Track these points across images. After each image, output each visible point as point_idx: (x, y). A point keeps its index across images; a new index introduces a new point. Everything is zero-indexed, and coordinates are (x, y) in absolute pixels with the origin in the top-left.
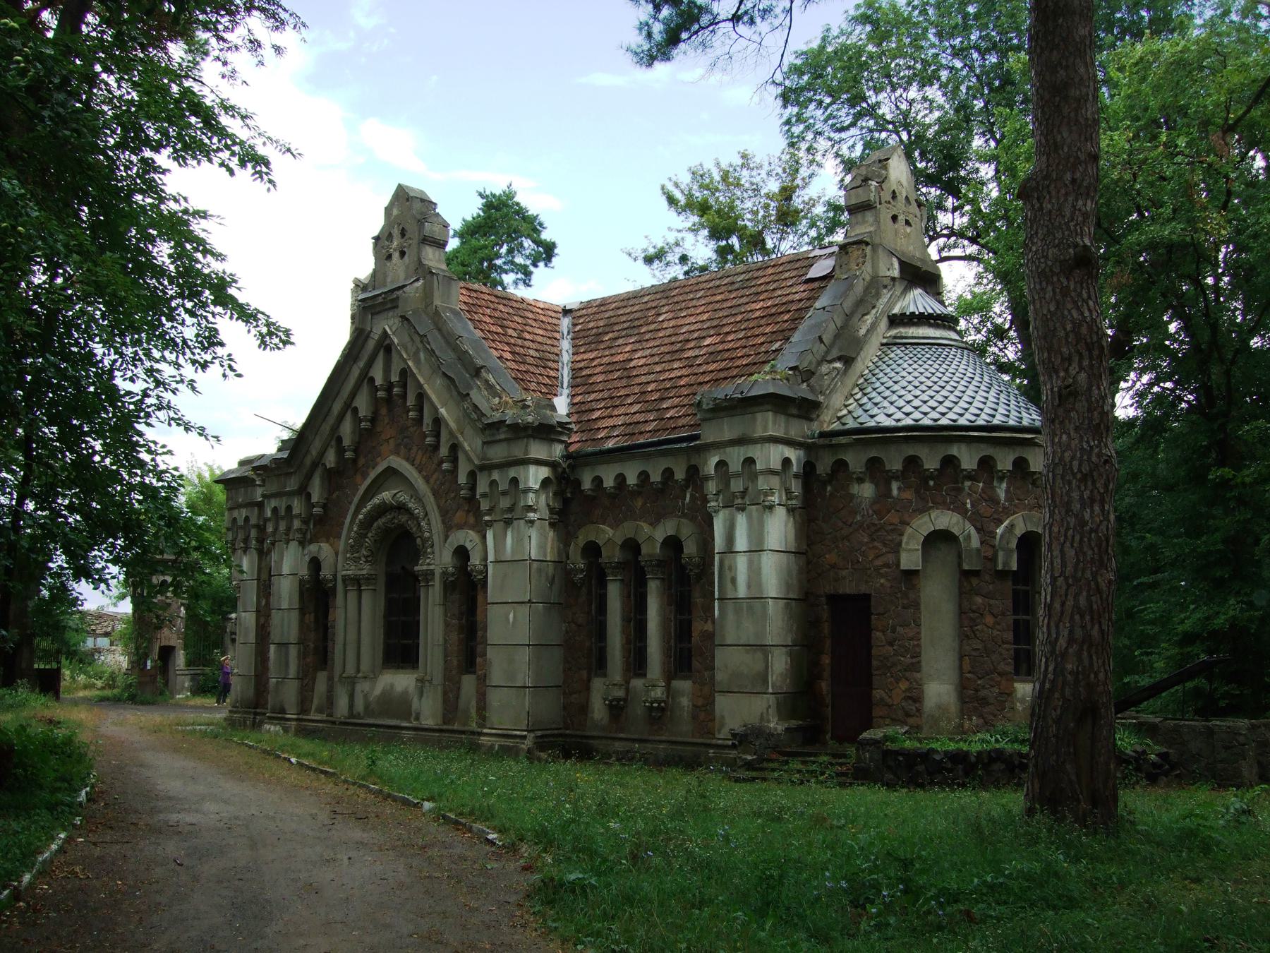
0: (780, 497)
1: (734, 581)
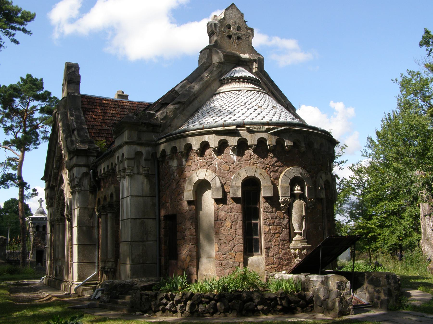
0: (138, 169)
1: (123, 210)
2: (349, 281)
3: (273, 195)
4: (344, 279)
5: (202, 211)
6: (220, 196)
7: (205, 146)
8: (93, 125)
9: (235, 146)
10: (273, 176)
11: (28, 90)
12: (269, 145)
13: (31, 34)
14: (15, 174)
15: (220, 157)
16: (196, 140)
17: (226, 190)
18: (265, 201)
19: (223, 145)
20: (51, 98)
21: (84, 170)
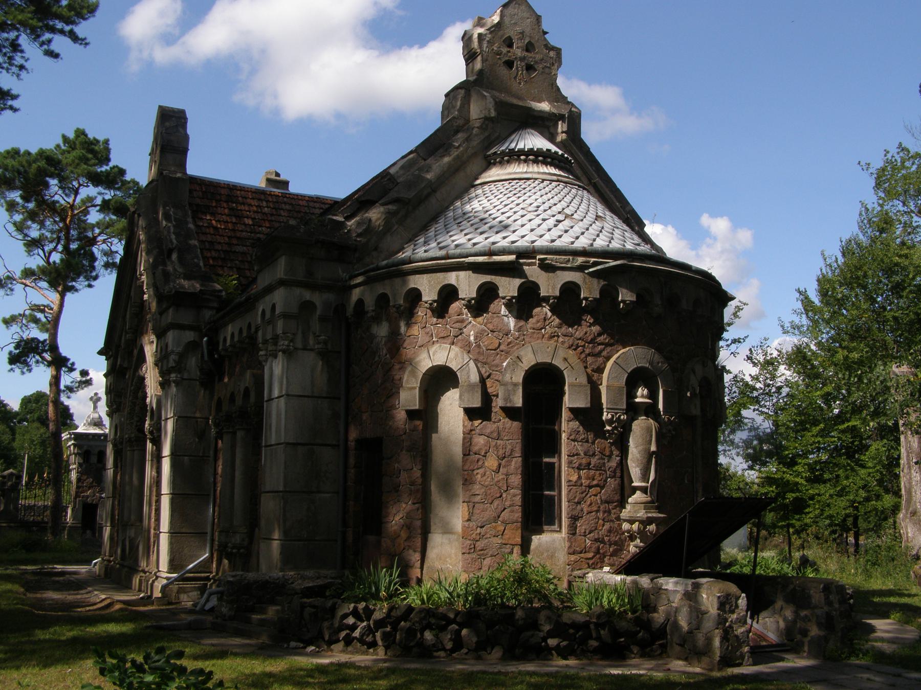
2: (743, 595)
3: (589, 405)
4: (733, 588)
5: (437, 432)
6: (476, 403)
7: (449, 294)
8: (211, 243)
9: (513, 297)
10: (591, 365)
11: (77, 161)
12: (586, 299)
13: (87, 44)
14: (45, 340)
15: (480, 319)
16: (430, 282)
17: (490, 390)
18: (572, 416)
19: (487, 294)
20: (125, 183)
21: (190, 336)
